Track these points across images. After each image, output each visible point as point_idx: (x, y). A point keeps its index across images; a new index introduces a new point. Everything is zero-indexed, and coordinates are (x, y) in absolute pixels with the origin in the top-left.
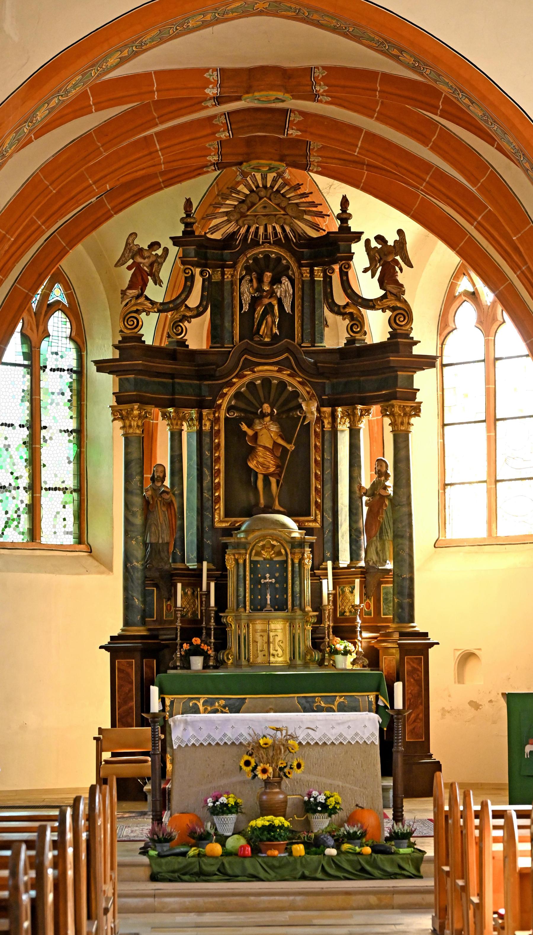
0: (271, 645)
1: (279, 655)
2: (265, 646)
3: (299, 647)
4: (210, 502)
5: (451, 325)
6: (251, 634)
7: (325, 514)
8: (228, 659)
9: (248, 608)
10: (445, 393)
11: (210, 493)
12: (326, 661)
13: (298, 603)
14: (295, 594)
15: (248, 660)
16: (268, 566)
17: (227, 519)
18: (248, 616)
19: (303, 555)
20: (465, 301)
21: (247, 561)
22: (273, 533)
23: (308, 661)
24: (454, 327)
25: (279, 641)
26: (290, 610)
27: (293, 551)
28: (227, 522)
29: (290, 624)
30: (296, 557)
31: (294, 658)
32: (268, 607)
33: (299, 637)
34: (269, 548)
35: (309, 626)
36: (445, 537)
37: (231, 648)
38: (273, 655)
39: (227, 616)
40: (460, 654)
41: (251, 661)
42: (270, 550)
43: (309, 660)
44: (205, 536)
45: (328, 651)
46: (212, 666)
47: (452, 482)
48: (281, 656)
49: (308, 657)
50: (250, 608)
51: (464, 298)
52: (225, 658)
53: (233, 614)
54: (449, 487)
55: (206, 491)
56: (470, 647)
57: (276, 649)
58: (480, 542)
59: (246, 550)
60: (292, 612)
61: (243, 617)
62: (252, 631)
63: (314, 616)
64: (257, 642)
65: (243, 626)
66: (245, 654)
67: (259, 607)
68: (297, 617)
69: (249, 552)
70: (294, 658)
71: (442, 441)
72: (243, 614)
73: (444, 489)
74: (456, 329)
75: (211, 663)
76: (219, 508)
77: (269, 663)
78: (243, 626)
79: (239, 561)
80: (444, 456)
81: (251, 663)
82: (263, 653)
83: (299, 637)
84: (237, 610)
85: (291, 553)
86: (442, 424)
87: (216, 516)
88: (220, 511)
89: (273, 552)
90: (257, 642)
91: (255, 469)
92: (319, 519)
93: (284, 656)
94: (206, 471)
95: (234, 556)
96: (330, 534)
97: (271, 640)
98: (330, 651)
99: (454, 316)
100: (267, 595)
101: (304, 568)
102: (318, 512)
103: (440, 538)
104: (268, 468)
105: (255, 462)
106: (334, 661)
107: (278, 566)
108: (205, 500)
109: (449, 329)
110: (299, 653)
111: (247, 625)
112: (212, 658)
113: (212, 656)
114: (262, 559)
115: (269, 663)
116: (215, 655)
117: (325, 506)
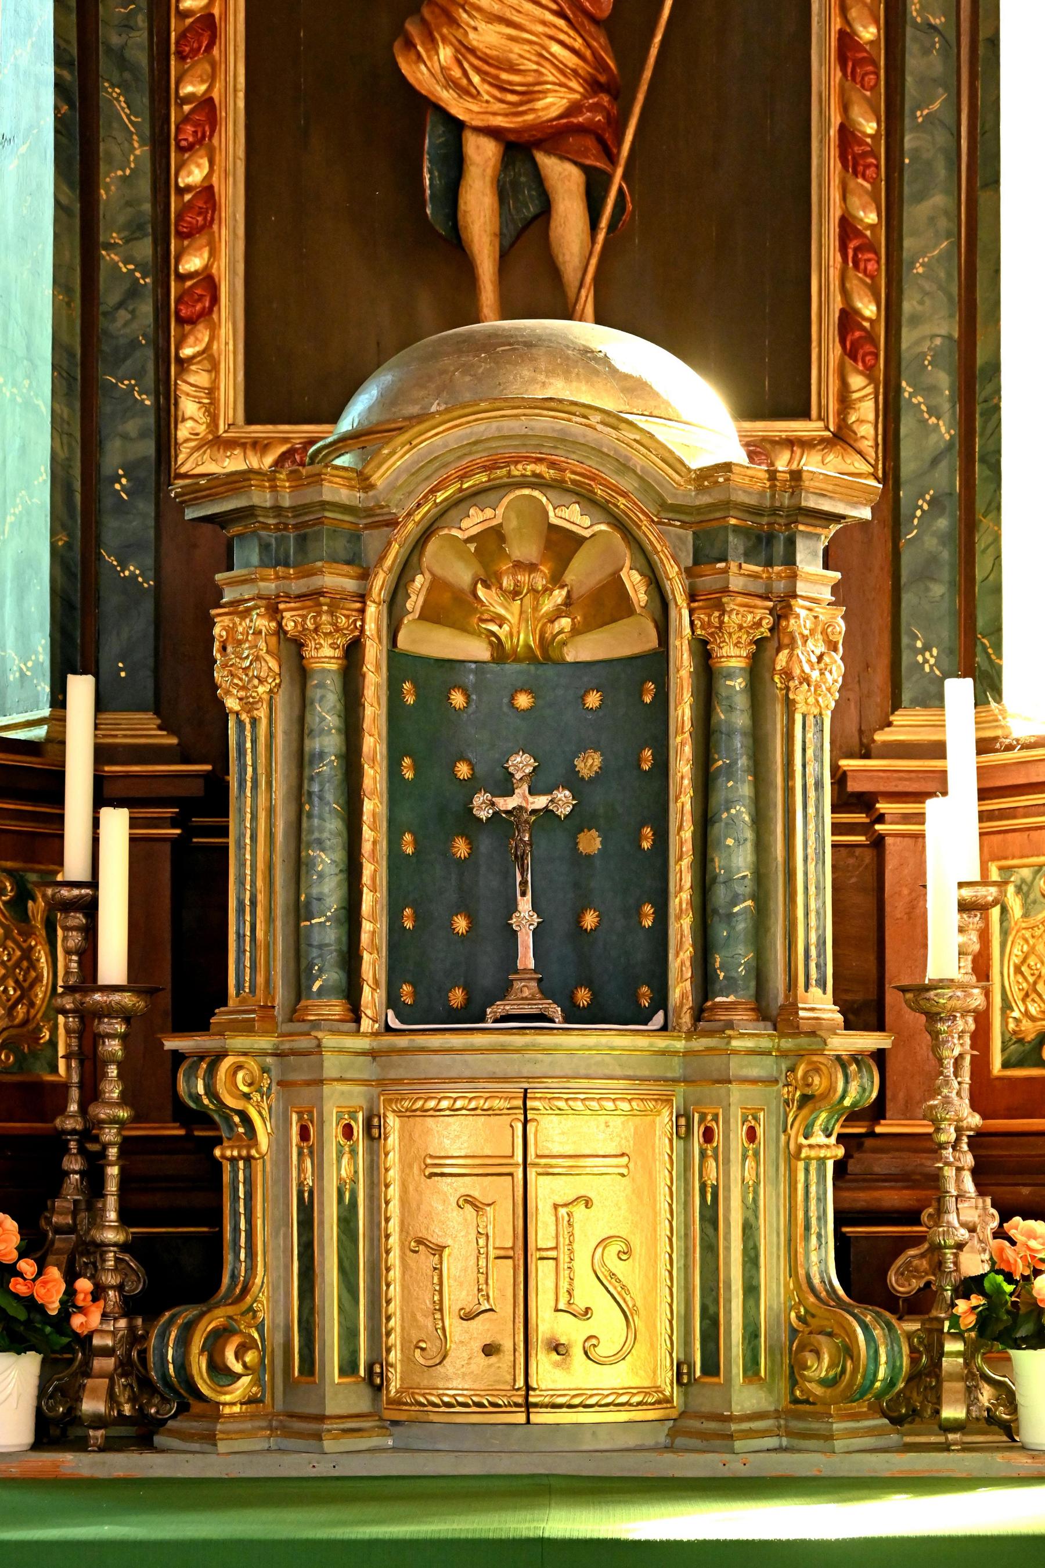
0: (543, 1273)
1: (604, 1350)
2: (503, 1274)
3: (751, 1290)
4: (146, 308)
6: (393, 1192)
7: (907, 389)
8: (219, 1371)
9: (372, 997)
11: (145, 249)
12: (952, 1388)
13: (743, 957)
14: (720, 895)
15: (375, 1383)
16: (523, 701)
17: (258, 430)
18: (373, 1054)
19: (782, 611)
21: (374, 653)
22: (563, 440)
23: (818, 1390)
25: (604, 1242)
26: (686, 1019)
27: (707, 581)
28: (260, 446)
29: (684, 1115)
30: (732, 620)
31: (711, 1367)
32: (526, 988)
33: (752, 1209)
34: (532, 568)
35: (819, 1138)
37: (245, 1290)
38: (557, 1348)
39: (220, 1056)
41: (394, 1386)
42: (540, 582)
43: (823, 1382)
44: (113, 529)
45: (971, 1320)
46: (98, 1421)
48: (620, 1356)
49: (820, 1367)
50: (393, 1001)
52: (199, 1365)
53: (265, 1043)
55: (115, 237)
57: (581, 1302)
59: (365, 576)
60: (690, 1035)
61: (331, 1065)
62: (406, 1166)
63: (856, 1058)
64: (439, 1250)
65: (333, 1132)
66: (350, 1334)
67: (457, 997)
68: (736, 1067)
69: (380, 583)
70: (711, 1367)
72: (329, 1041)
75: (92, 1405)
76: (209, 358)
77: (528, 1406)
78: (333, 1132)
79: (309, 652)
81: (399, 1402)
82: (481, 1330)
83: (752, 1209)
84: (294, 1014)
85: (692, 597)
87: (189, 407)
88: (214, 368)
89: (559, 596)
90: (439, 1250)
91: (447, 98)
92: (866, 430)
93: (641, 1349)
94: (121, 105)
95: (274, 612)
96: (942, 523)
97: (543, 1235)
98: (984, 1321)
100: (513, 907)
101: (790, 705)
102: (856, 381)
104: (529, 95)
105: (445, 54)
106: (1008, 1397)
107: (593, 700)
108: (110, 296)
110: (751, 1334)
111: (368, 1126)
112: (106, 1364)
113: (106, 1352)
114: (478, 650)
115: (528, 1406)
116: (133, 1338)
117: (908, 337)
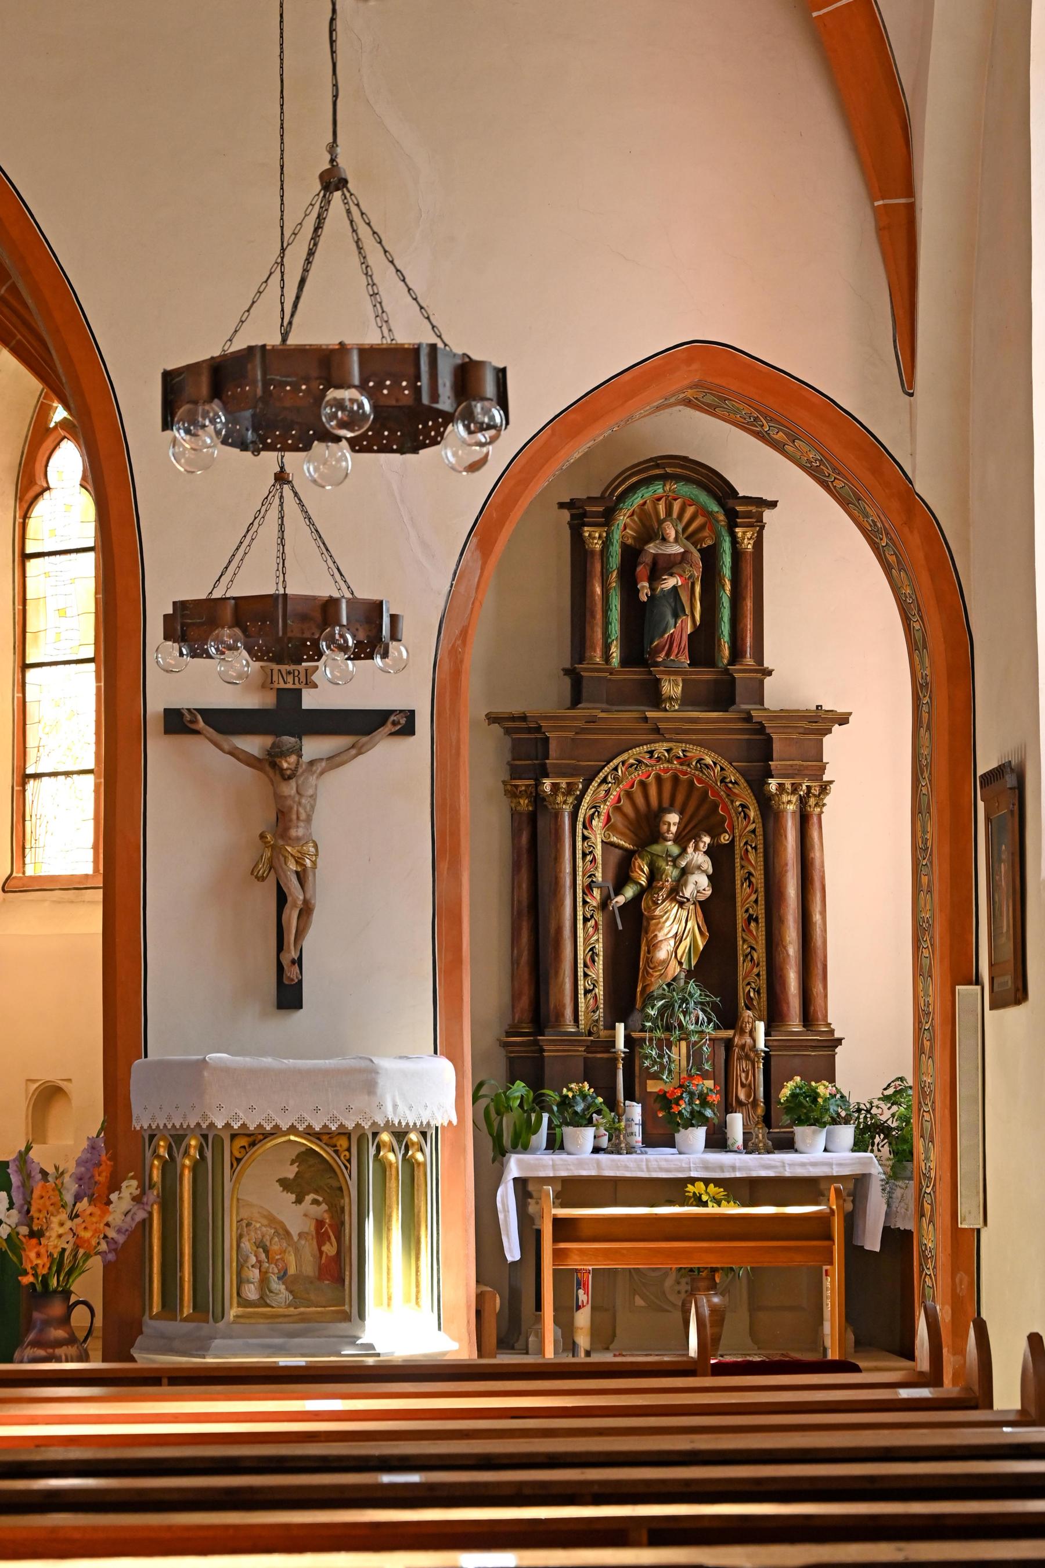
5: (39, 483)
10: (27, 607)
20: (64, 437)
24: (45, 485)
36: (24, 873)
40: (37, 1088)
47: (39, 771)
51: (63, 433)
54: (32, 781)
56: (53, 1076)
58: (79, 883)
71: (21, 695)
73: (23, 784)
74: (48, 488)
80: (25, 724)
86: (21, 664)
99: (47, 466)
103: (14, 875)
109: (36, 489)
